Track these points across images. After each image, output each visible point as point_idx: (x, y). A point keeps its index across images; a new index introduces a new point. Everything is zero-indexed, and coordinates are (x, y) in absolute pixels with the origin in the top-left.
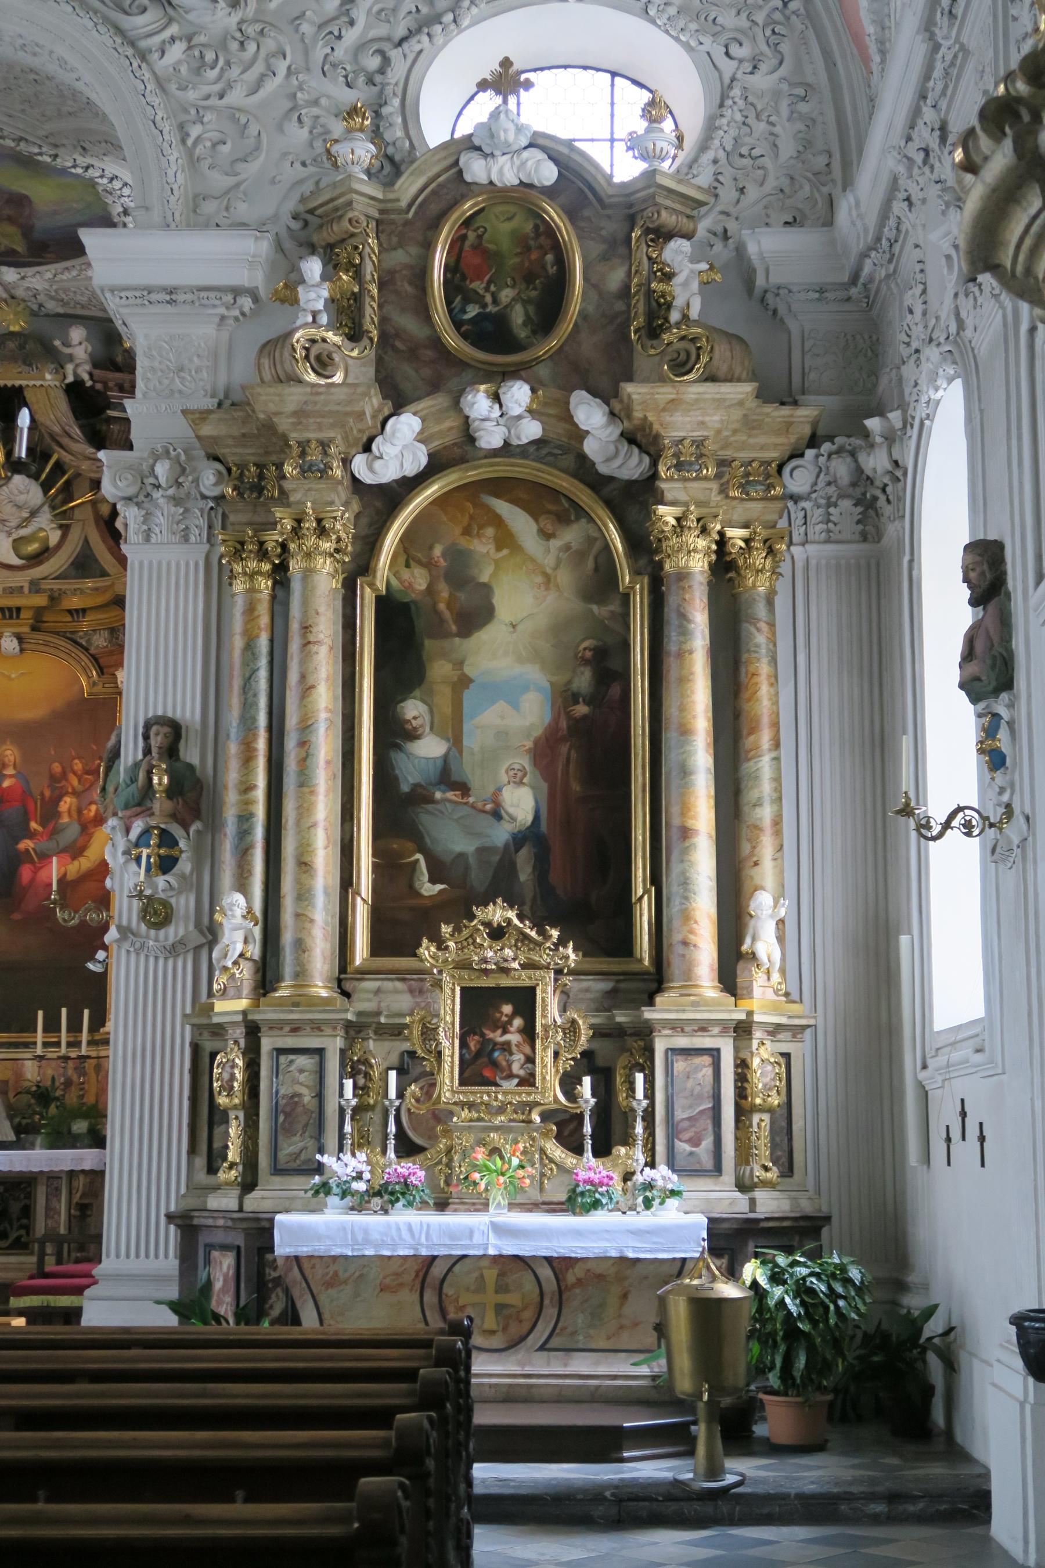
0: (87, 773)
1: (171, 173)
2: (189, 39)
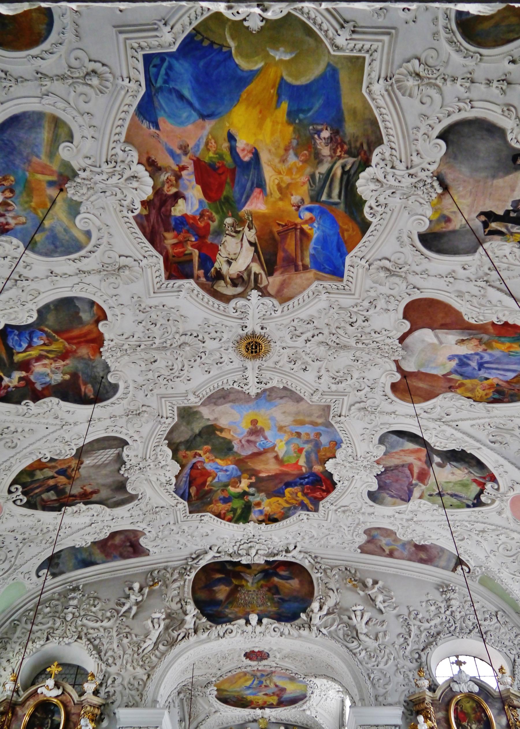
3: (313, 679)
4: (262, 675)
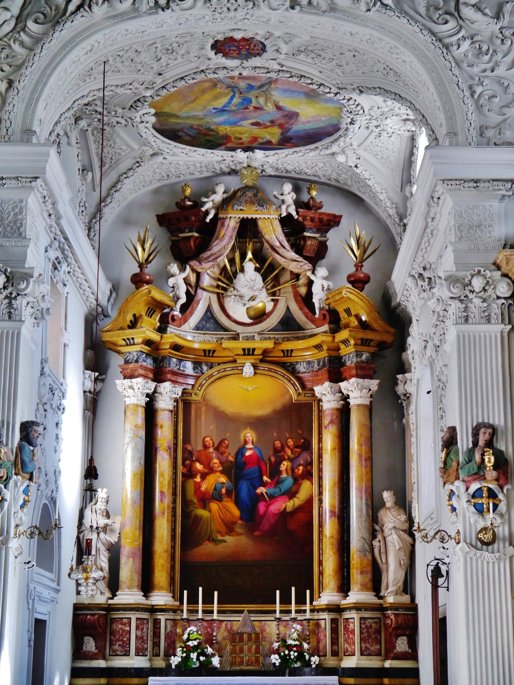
0: (297, 447)
1: (469, 114)
2: (472, 39)
3: (355, 96)
4: (250, 87)
